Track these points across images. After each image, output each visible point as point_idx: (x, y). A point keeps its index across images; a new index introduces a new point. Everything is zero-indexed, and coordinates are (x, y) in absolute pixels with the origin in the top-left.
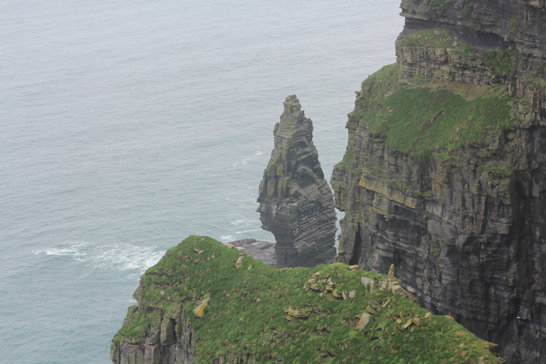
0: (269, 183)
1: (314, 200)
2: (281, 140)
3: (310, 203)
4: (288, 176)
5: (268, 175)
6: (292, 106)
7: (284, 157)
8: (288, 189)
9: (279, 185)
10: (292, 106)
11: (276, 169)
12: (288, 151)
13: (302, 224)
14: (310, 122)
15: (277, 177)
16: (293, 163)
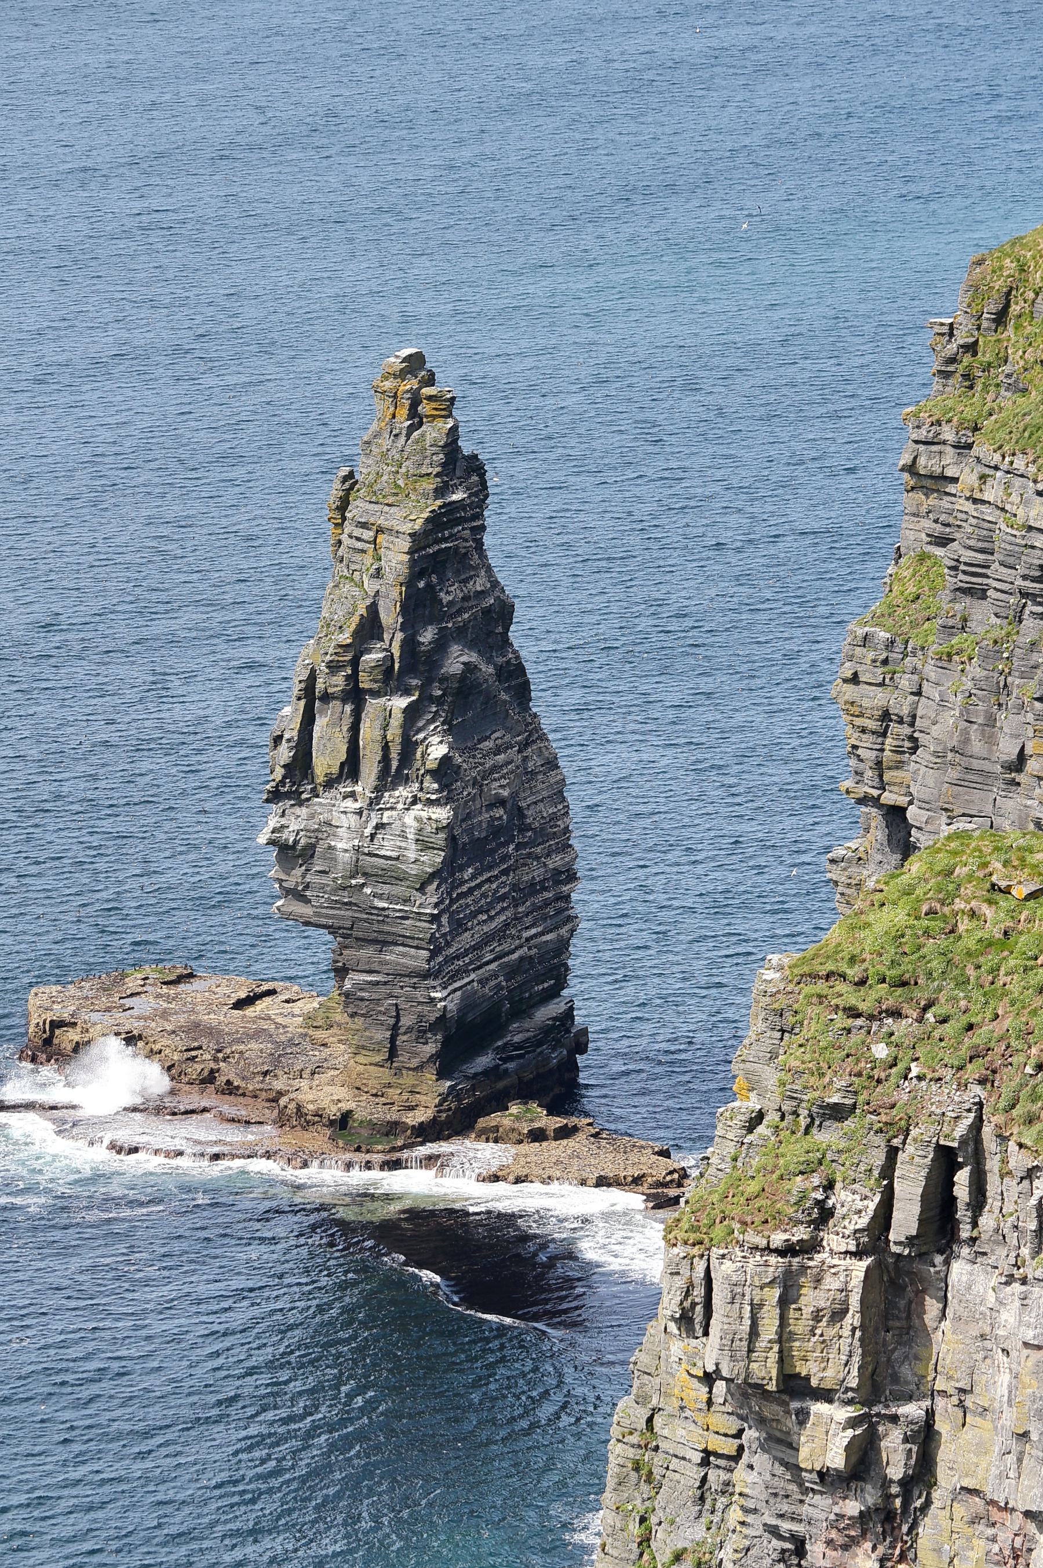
0: (320, 724)
1: (505, 793)
2: (375, 542)
3: (491, 806)
4: (407, 692)
5: (320, 685)
6: (418, 394)
7: (390, 616)
8: (409, 747)
9: (369, 731)
10: (418, 394)
11: (355, 663)
12: (410, 583)
13: (461, 896)
14: (475, 467)
15: (355, 696)
16: (427, 636)
